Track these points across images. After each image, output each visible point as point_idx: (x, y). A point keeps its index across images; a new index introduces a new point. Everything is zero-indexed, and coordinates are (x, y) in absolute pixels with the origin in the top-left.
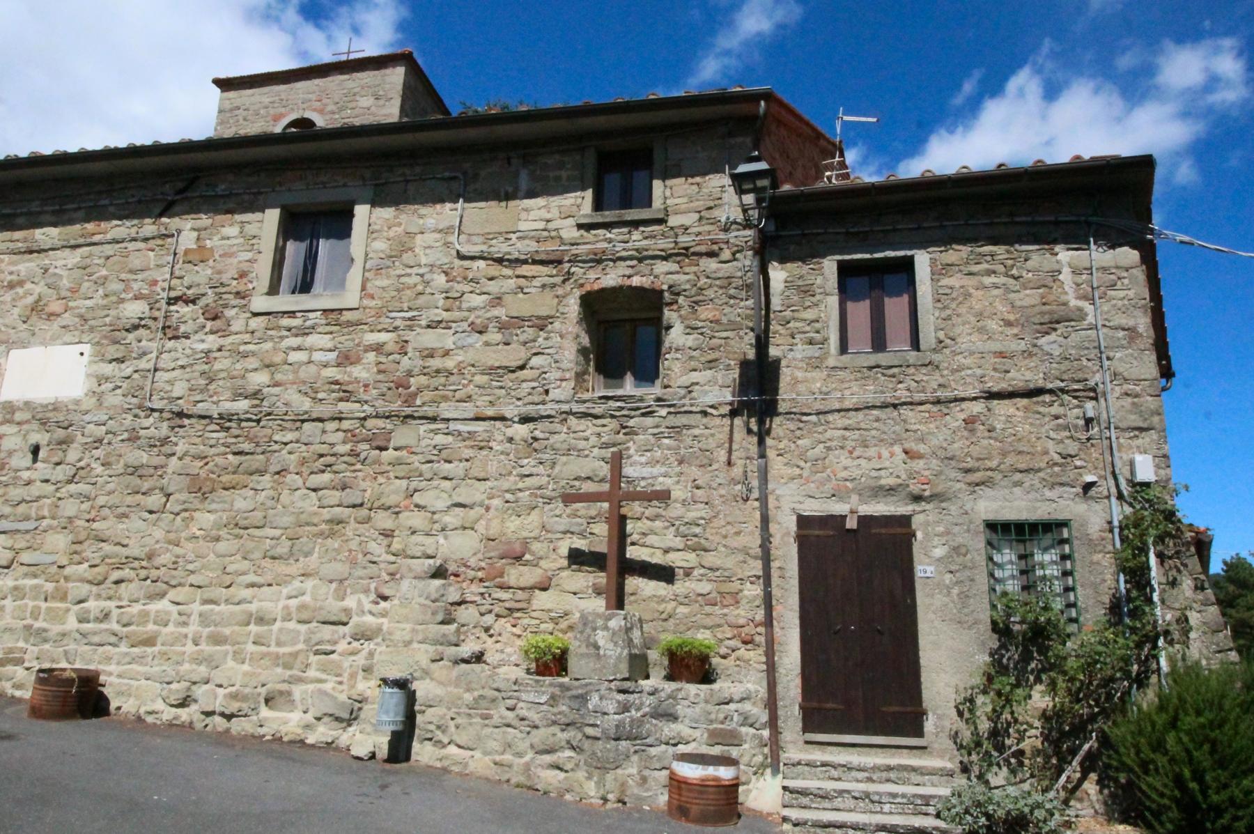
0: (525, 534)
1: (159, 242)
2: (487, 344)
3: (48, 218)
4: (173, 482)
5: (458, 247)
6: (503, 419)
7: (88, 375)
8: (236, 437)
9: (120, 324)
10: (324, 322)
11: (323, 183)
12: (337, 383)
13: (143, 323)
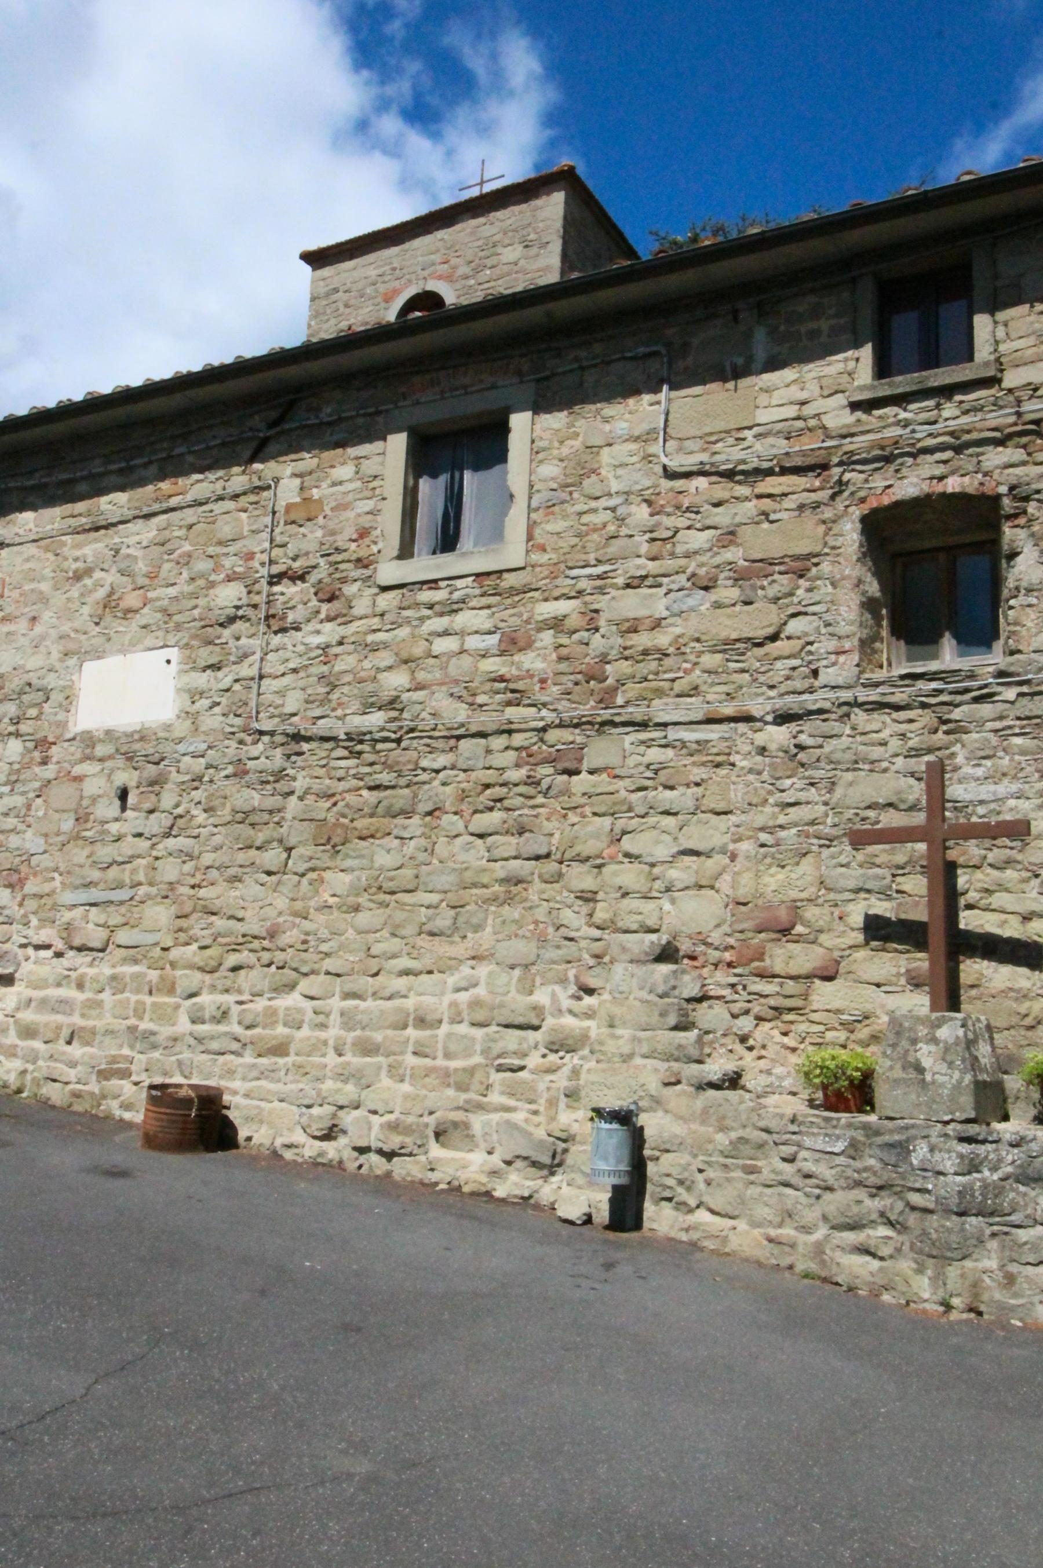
0: (794, 894)
1: (252, 498)
2: (718, 605)
3: (114, 479)
4: (296, 833)
5: (665, 460)
6: (748, 719)
7: (178, 691)
8: (372, 764)
9: (213, 617)
10: (477, 591)
11: (465, 387)
12: (502, 679)
13: (240, 613)
